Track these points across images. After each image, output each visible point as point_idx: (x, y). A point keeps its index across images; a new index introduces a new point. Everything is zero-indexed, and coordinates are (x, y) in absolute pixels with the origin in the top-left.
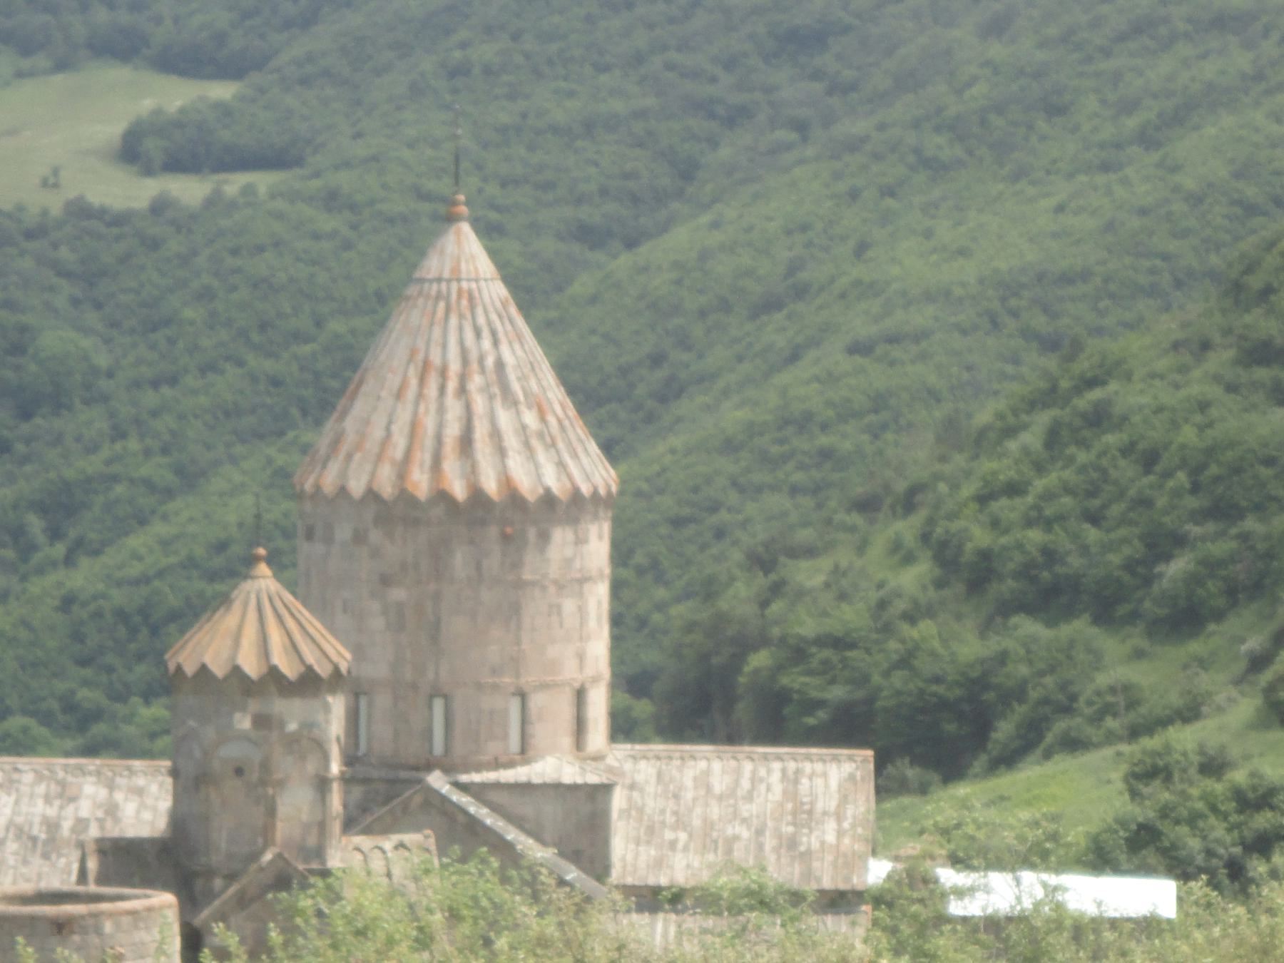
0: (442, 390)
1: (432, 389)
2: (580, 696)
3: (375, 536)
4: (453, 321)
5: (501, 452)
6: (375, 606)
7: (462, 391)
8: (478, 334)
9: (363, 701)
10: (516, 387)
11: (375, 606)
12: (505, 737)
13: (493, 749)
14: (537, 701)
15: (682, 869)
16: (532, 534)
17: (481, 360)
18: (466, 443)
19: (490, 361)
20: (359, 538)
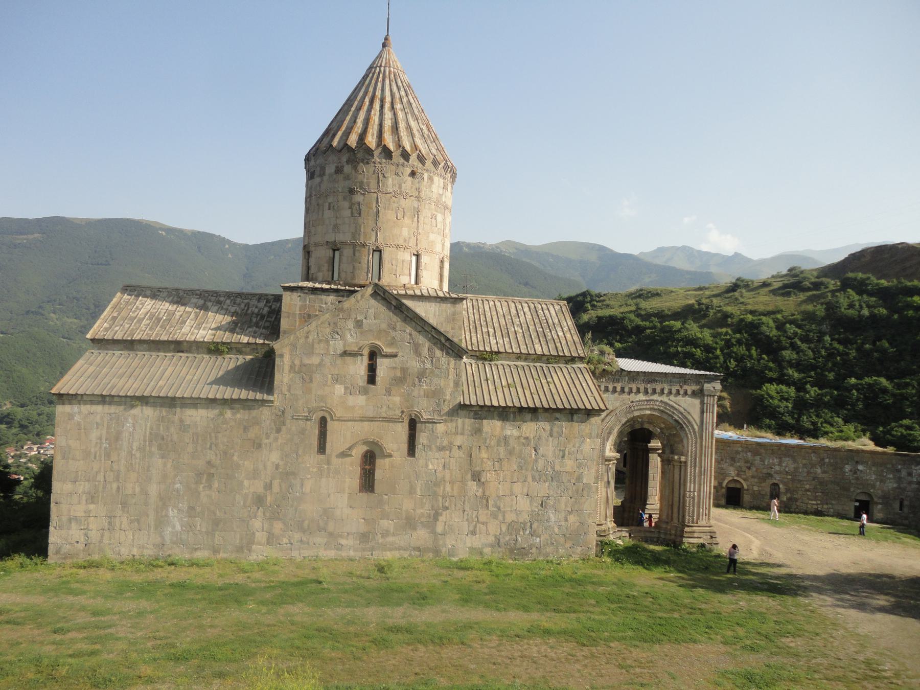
0: (382, 107)
1: (377, 106)
2: (442, 262)
3: (347, 169)
4: (387, 82)
5: (412, 135)
6: (346, 204)
7: (392, 107)
8: (399, 90)
9: (337, 253)
10: (416, 112)
11: (346, 204)
12: (410, 275)
13: (404, 280)
14: (424, 260)
15: (494, 344)
16: (426, 176)
17: (401, 98)
18: (395, 128)
19: (405, 100)
20: (339, 170)
